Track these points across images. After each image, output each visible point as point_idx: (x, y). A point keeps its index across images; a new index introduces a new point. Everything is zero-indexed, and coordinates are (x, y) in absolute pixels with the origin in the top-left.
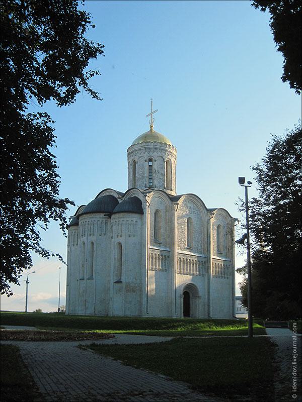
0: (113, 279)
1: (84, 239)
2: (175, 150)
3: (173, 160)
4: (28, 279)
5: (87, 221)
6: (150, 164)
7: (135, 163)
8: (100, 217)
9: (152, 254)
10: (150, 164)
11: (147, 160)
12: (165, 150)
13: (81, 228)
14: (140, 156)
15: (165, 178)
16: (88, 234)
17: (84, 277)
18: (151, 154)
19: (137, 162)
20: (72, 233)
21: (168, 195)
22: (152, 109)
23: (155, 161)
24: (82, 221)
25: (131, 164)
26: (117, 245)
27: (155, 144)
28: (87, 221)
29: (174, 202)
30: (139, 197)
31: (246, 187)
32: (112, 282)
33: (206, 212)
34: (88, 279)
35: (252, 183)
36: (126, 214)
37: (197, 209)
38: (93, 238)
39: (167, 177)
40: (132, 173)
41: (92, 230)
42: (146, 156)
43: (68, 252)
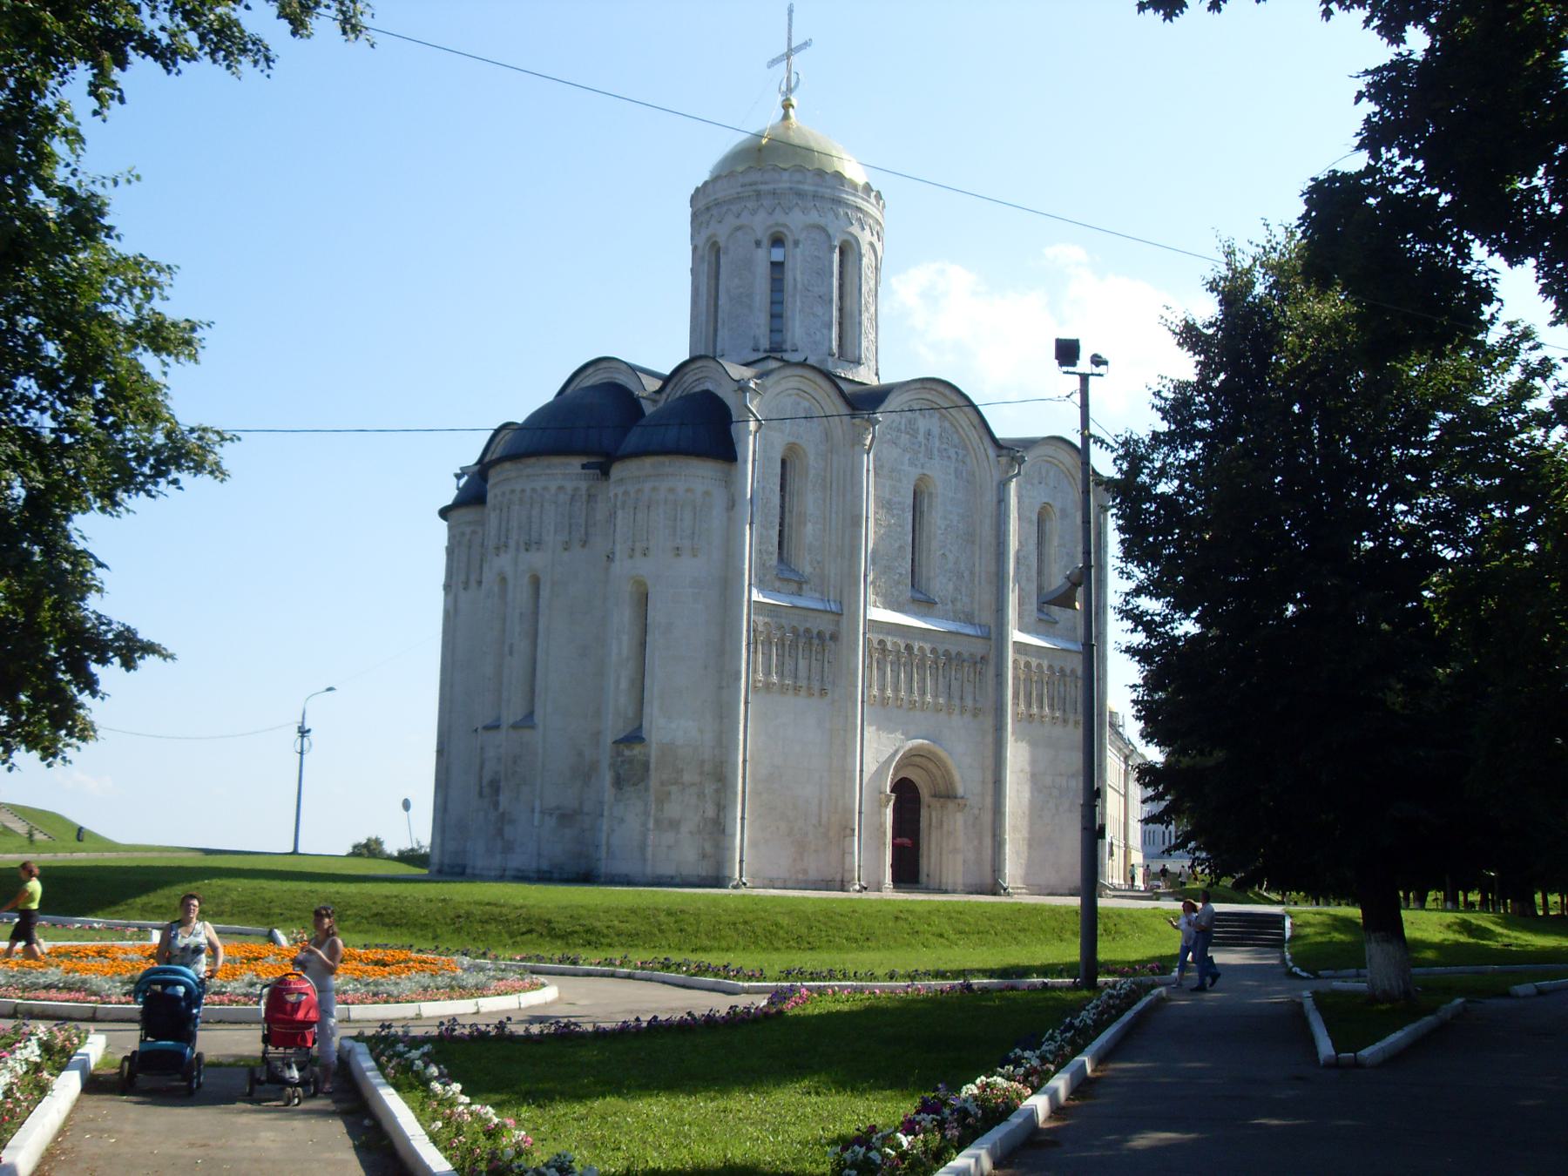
0: (613, 728)
1: (504, 562)
2: (879, 196)
3: (865, 237)
5: (518, 487)
6: (777, 254)
10: (777, 254)
11: (766, 242)
12: (839, 202)
14: (738, 222)
15: (835, 313)
16: (518, 544)
17: (499, 719)
18: (779, 217)
20: (463, 534)
22: (790, 39)
23: (796, 243)
25: (702, 257)
27: (798, 176)
28: (518, 487)
30: (720, 394)
31: (1084, 378)
32: (609, 739)
33: (991, 452)
34: (515, 726)
35: (1106, 363)
36: (667, 464)
39: (841, 310)
40: (703, 289)
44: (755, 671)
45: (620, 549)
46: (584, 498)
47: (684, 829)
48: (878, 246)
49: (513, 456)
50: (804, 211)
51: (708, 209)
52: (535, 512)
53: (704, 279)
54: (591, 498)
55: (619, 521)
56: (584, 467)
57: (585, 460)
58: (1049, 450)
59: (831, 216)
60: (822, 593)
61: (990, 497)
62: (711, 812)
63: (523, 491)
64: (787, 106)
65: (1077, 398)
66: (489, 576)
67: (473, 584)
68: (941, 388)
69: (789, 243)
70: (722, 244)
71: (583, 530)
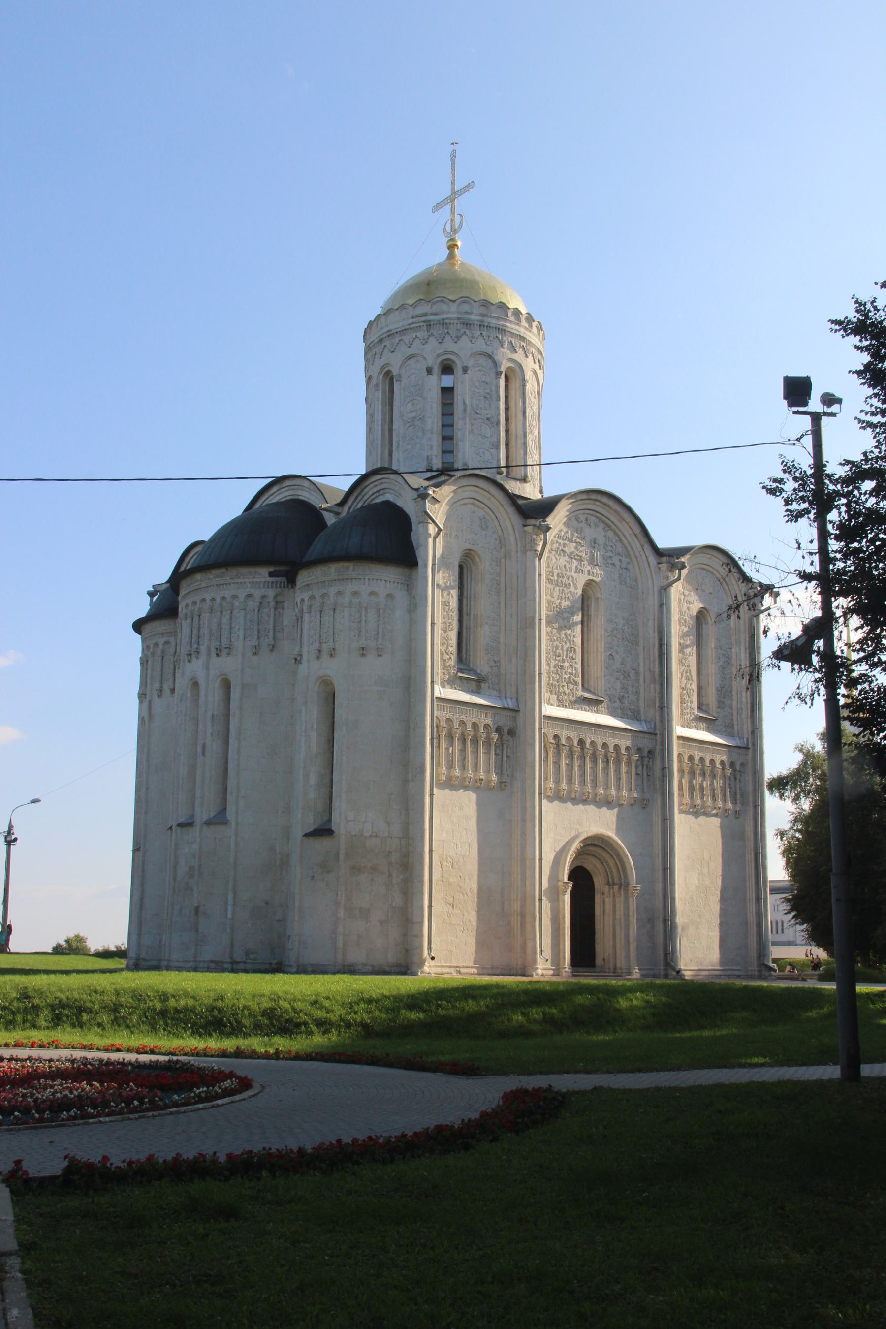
0: (304, 819)
1: (195, 668)
2: (540, 328)
3: (529, 365)
4: (11, 827)
5: (208, 597)
6: (447, 381)
8: (253, 584)
9: (448, 720)
10: (447, 381)
11: (436, 369)
12: (502, 330)
13: (184, 625)
14: (410, 351)
15: (503, 434)
17: (193, 816)
18: (449, 345)
19: (400, 375)
20: (156, 645)
21: (513, 499)
23: (465, 370)
24: (189, 601)
25: (377, 385)
27: (465, 307)
28: (208, 597)
29: (533, 521)
30: (400, 503)
31: (816, 418)
32: (298, 833)
33: (653, 559)
34: (208, 823)
35: (839, 401)
36: (351, 569)
37: (620, 549)
39: (507, 431)
40: (379, 416)
41: (225, 633)
43: (142, 721)
44: (438, 765)
45: (308, 651)
46: (272, 604)
48: (540, 373)
49: (202, 568)
50: (472, 339)
51: (381, 340)
52: (225, 620)
53: (378, 406)
54: (278, 605)
55: (306, 626)
56: (271, 575)
57: (272, 569)
58: (704, 558)
59: (496, 343)
60: (499, 691)
61: (652, 602)
62: (398, 901)
63: (213, 599)
64: (452, 247)
65: (808, 441)
66: (182, 683)
67: (167, 691)
68: (605, 499)
69: (458, 370)
70: (395, 372)
71: (271, 634)
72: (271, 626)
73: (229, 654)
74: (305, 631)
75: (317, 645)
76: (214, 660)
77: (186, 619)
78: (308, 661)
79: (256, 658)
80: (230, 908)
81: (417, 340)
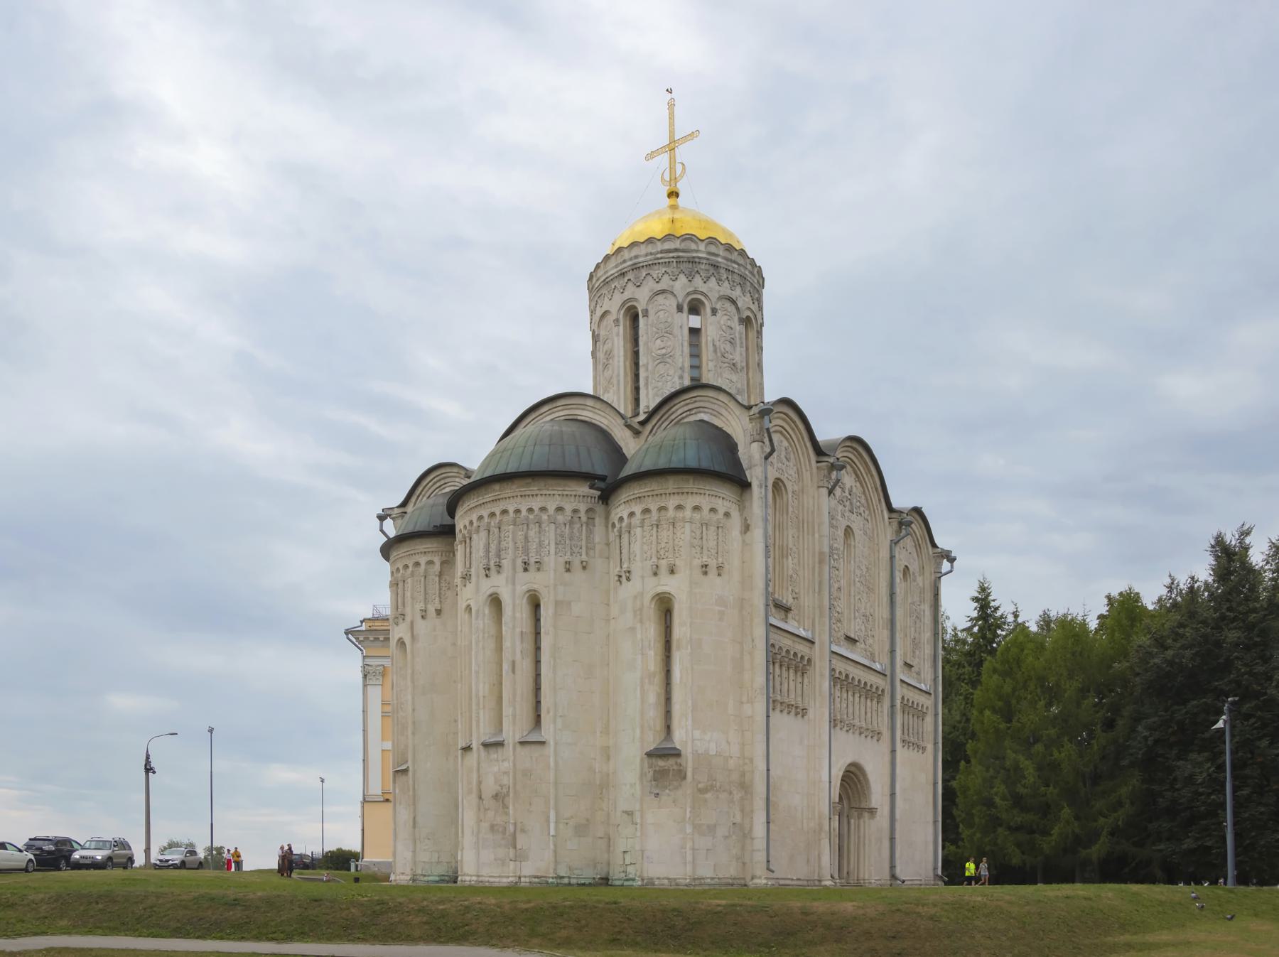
6: (695, 321)
7: (637, 315)
10: (695, 321)
11: (686, 308)
16: (514, 561)
23: (714, 312)
25: (617, 320)
26: (651, 612)
36: (690, 484)
38: (536, 580)
42: (681, 286)
46: (584, 519)
47: (722, 831)
63: (518, 511)
64: (673, 194)
72: (584, 543)
73: (539, 569)
74: (636, 547)
75: (654, 559)
76: (521, 575)
77: (477, 531)
78: (643, 577)
79: (567, 575)
80: (552, 826)
81: (666, 276)
